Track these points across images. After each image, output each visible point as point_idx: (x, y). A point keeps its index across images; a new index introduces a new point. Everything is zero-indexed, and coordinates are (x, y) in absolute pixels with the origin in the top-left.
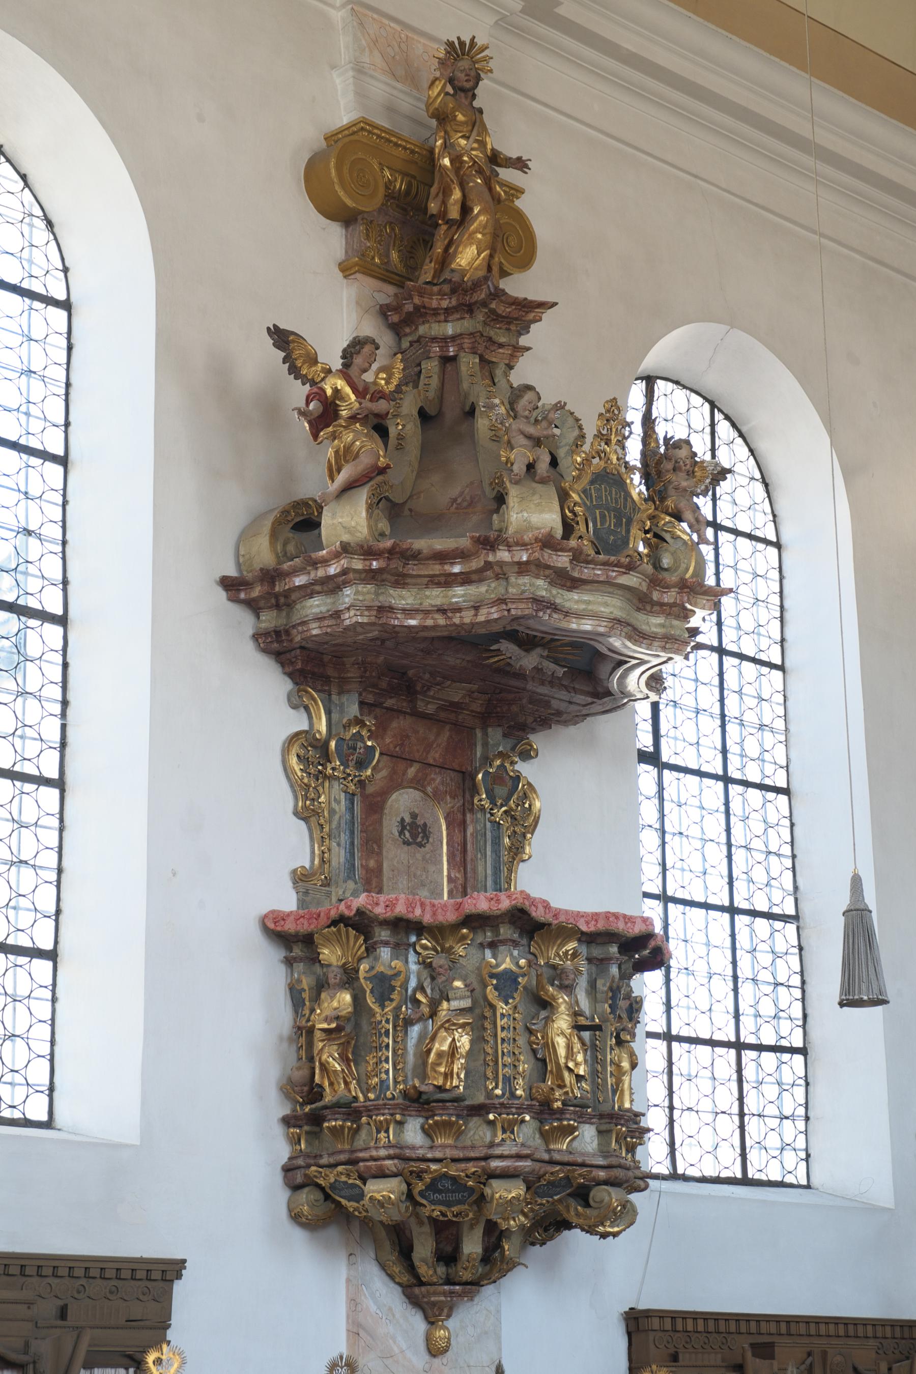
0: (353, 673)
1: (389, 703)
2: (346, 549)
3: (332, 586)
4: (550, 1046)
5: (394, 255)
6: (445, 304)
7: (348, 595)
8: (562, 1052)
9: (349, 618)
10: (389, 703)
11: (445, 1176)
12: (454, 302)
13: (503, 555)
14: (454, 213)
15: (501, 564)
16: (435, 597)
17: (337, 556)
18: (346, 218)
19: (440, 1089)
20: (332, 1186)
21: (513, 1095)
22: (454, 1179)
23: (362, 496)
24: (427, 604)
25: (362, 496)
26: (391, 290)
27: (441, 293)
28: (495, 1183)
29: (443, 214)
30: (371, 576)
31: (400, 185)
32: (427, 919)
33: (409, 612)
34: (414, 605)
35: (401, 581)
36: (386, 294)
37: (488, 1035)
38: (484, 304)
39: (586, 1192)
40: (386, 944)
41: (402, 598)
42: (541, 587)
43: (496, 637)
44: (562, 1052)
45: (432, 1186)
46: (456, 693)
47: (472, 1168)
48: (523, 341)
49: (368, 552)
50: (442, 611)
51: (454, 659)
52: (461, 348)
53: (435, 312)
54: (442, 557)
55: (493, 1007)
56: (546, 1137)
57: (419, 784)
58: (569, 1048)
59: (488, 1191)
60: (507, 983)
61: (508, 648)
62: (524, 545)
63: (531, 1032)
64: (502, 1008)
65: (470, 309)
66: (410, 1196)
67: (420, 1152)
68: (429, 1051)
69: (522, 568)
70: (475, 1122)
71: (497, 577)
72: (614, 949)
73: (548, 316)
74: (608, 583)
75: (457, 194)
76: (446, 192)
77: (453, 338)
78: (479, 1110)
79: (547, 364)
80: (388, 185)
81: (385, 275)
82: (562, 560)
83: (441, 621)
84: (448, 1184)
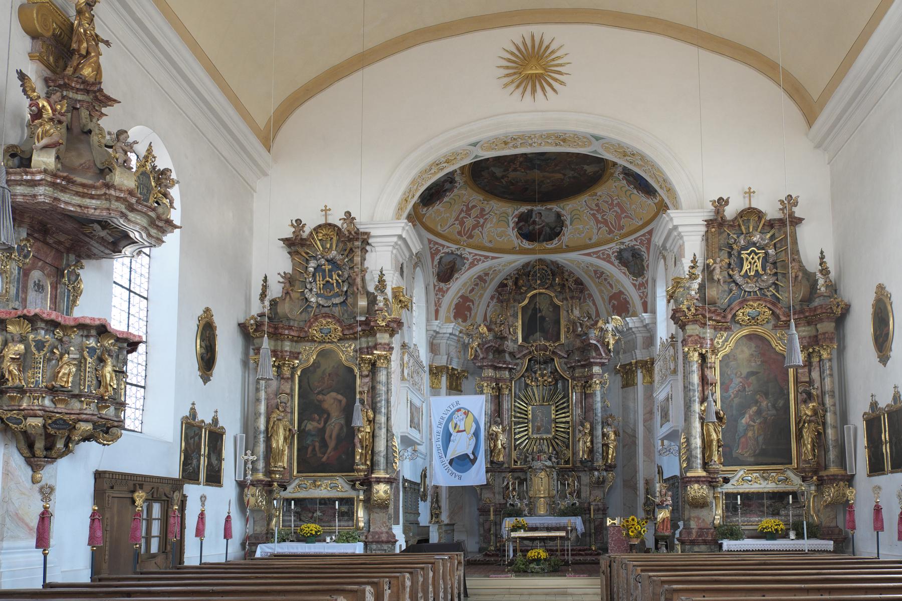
0: (27, 220)
1: (36, 235)
2: (45, 171)
3: (33, 184)
4: (104, 376)
5: (51, 59)
6: (78, 86)
7: (41, 190)
8: (108, 379)
9: (41, 199)
10: (36, 235)
11: (61, 419)
12: (82, 87)
13: (112, 192)
14: (84, 52)
15: (110, 195)
16: (77, 200)
17: (40, 172)
18: (34, 36)
19: (62, 386)
20: (7, 419)
21: (91, 392)
22: (64, 421)
23: (53, 152)
24: (73, 202)
25: (53, 152)
26: (49, 72)
27: (77, 82)
28: (81, 423)
29: (78, 51)
30: (53, 185)
31: (57, 32)
32: (62, 323)
33: (66, 203)
34: (70, 202)
35: (64, 189)
36: (47, 73)
37: (82, 369)
38: (95, 92)
39: (107, 430)
40: (43, 329)
41: (65, 197)
42: (122, 208)
43: (93, 221)
44: (108, 379)
45: (55, 422)
46: (62, 238)
47: (73, 417)
48: (104, 110)
49: (55, 176)
50: (80, 206)
51: (70, 226)
52: (82, 106)
53: (72, 88)
54: (84, 186)
55: (86, 360)
56: (99, 409)
57: (42, 269)
58: (111, 378)
59: (77, 426)
60: (92, 351)
61: (97, 227)
62: (121, 190)
63: (96, 370)
64: (89, 360)
65: (88, 92)
66: (44, 426)
67: (51, 409)
68: (59, 372)
69: (118, 199)
70: (74, 400)
71: (106, 199)
72: (126, 345)
73: (116, 105)
74: (145, 214)
75: (85, 45)
76: (80, 42)
77: (80, 101)
78: (77, 396)
79: (109, 121)
80: (54, 29)
81: (48, 66)
82: (133, 200)
83: (79, 210)
84: (61, 422)
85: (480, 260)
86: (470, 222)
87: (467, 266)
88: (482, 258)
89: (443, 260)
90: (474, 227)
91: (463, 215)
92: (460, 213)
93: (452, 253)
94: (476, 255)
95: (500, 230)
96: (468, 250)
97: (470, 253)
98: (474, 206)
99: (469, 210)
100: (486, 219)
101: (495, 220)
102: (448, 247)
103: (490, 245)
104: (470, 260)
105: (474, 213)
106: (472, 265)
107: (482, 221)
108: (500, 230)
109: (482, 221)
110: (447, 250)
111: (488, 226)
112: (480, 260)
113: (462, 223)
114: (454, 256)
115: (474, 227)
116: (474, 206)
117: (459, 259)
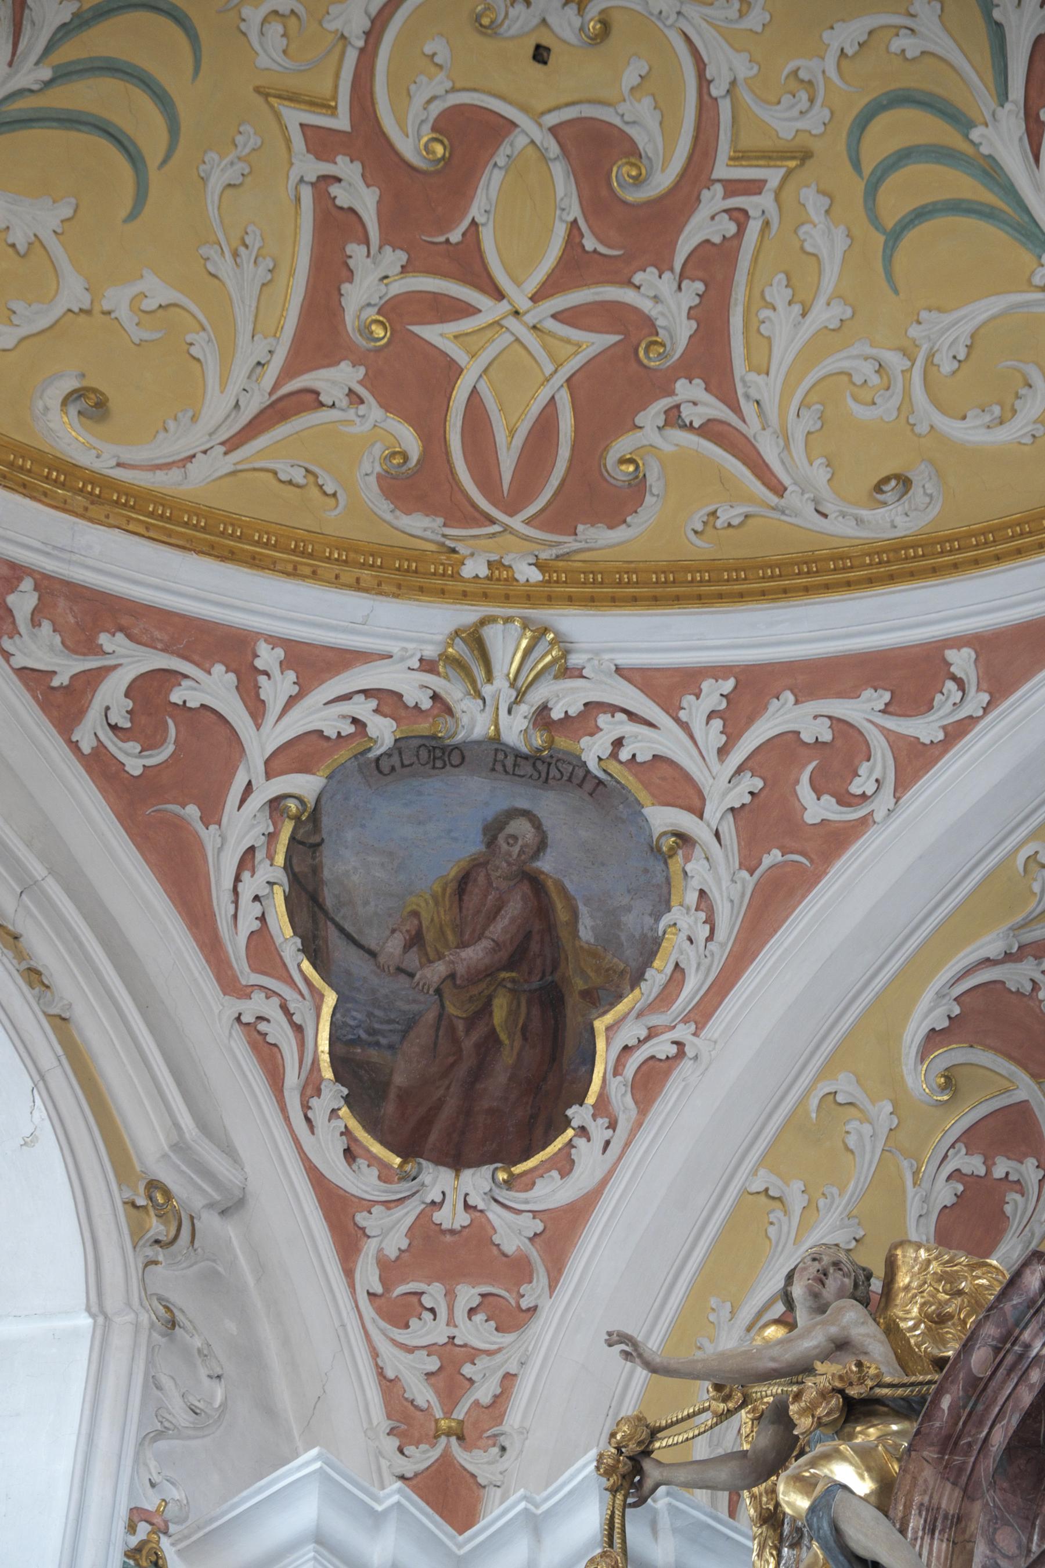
85: (844, 749)
86: (514, 355)
87: (716, 873)
88: (863, 709)
89: (346, 866)
90: (615, 390)
91: (374, 279)
92: (329, 274)
93: (431, 753)
94: (753, 687)
95: (948, 332)
96: (613, 638)
97: (670, 686)
98: (471, 134)
99: (427, 204)
100: (714, 264)
101: (826, 240)
102: (312, 663)
103: (895, 521)
104: (724, 789)
105: (523, 212)
106: (790, 850)
107: (666, 301)
108: (948, 332)
109: (666, 301)
110: (320, 714)
111: (786, 333)
112: (844, 749)
113: (414, 381)
114: (473, 799)
115: (615, 390)
116: (471, 134)
117: (552, 807)
